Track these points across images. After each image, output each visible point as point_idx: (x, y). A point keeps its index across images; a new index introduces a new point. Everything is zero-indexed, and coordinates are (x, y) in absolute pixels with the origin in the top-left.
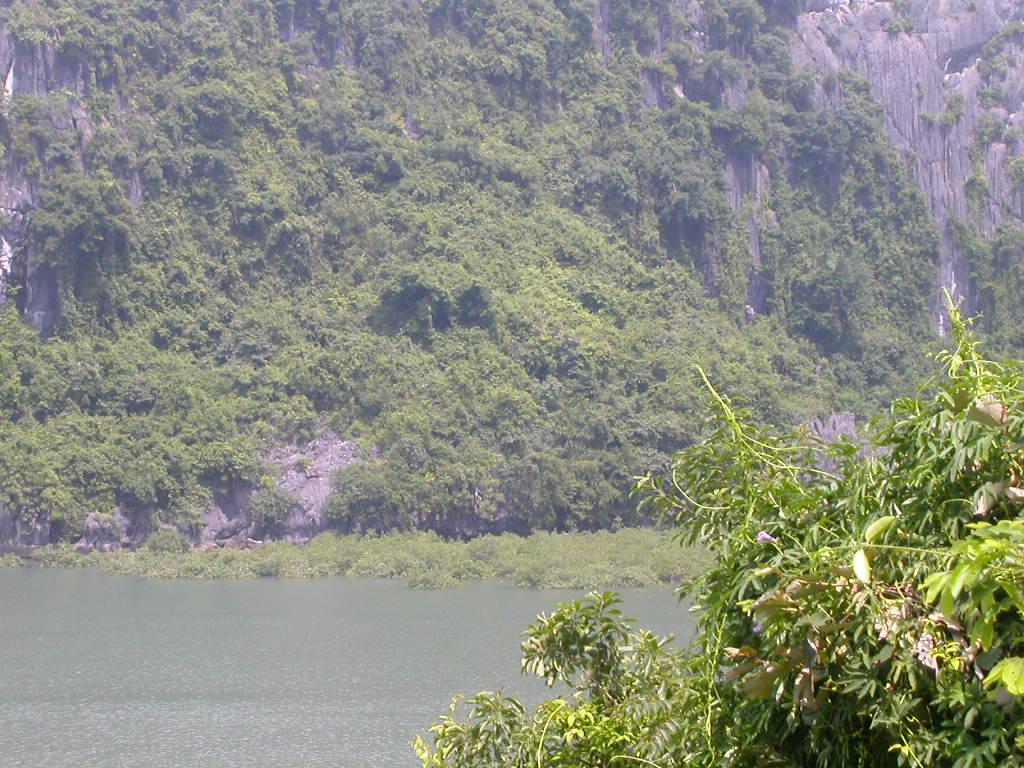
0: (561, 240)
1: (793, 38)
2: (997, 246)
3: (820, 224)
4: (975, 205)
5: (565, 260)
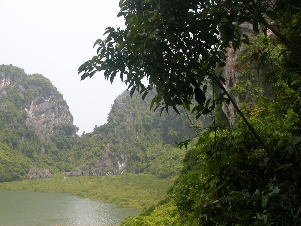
0: (3, 147)
1: (26, 121)
2: (48, 145)
3: (29, 143)
5: (3, 149)
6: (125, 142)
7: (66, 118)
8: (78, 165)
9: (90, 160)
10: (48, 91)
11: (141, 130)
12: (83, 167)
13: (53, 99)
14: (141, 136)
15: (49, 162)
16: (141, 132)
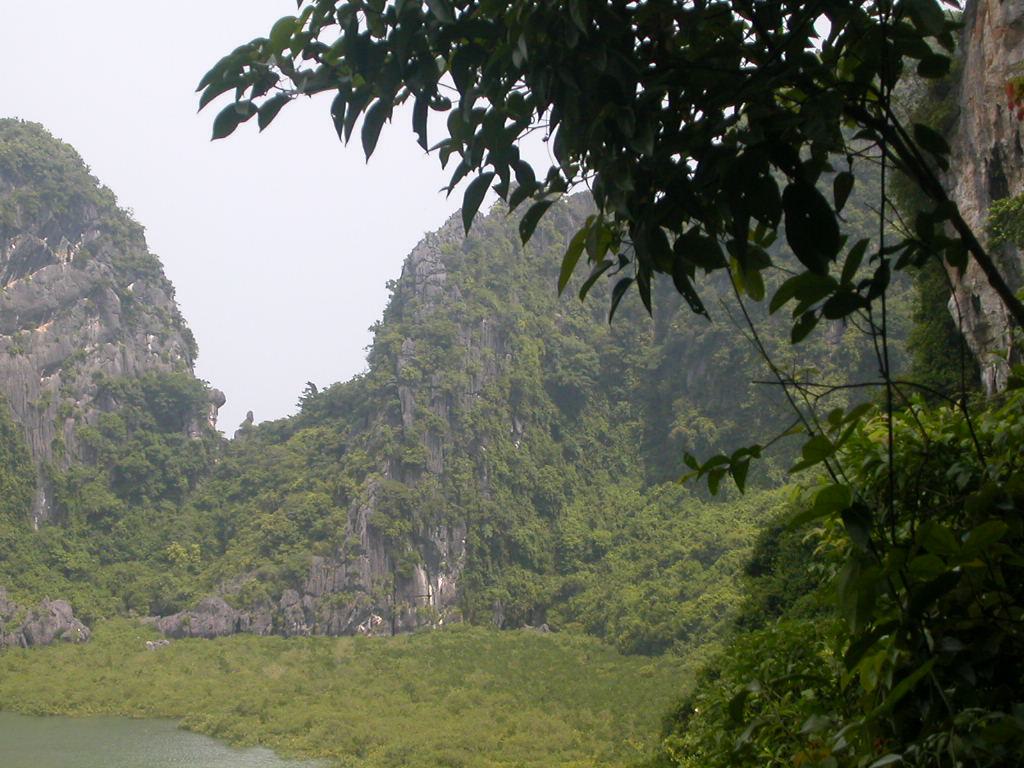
2: (70, 479)
4: (57, 454)
6: (456, 471)
7: (162, 344)
8: (218, 581)
9: (278, 557)
10: (68, 207)
11: (536, 410)
12: (244, 592)
13: (93, 249)
14: (536, 438)
15: (72, 564)
16: (534, 420)
